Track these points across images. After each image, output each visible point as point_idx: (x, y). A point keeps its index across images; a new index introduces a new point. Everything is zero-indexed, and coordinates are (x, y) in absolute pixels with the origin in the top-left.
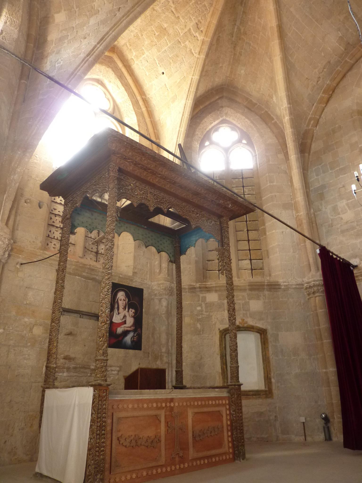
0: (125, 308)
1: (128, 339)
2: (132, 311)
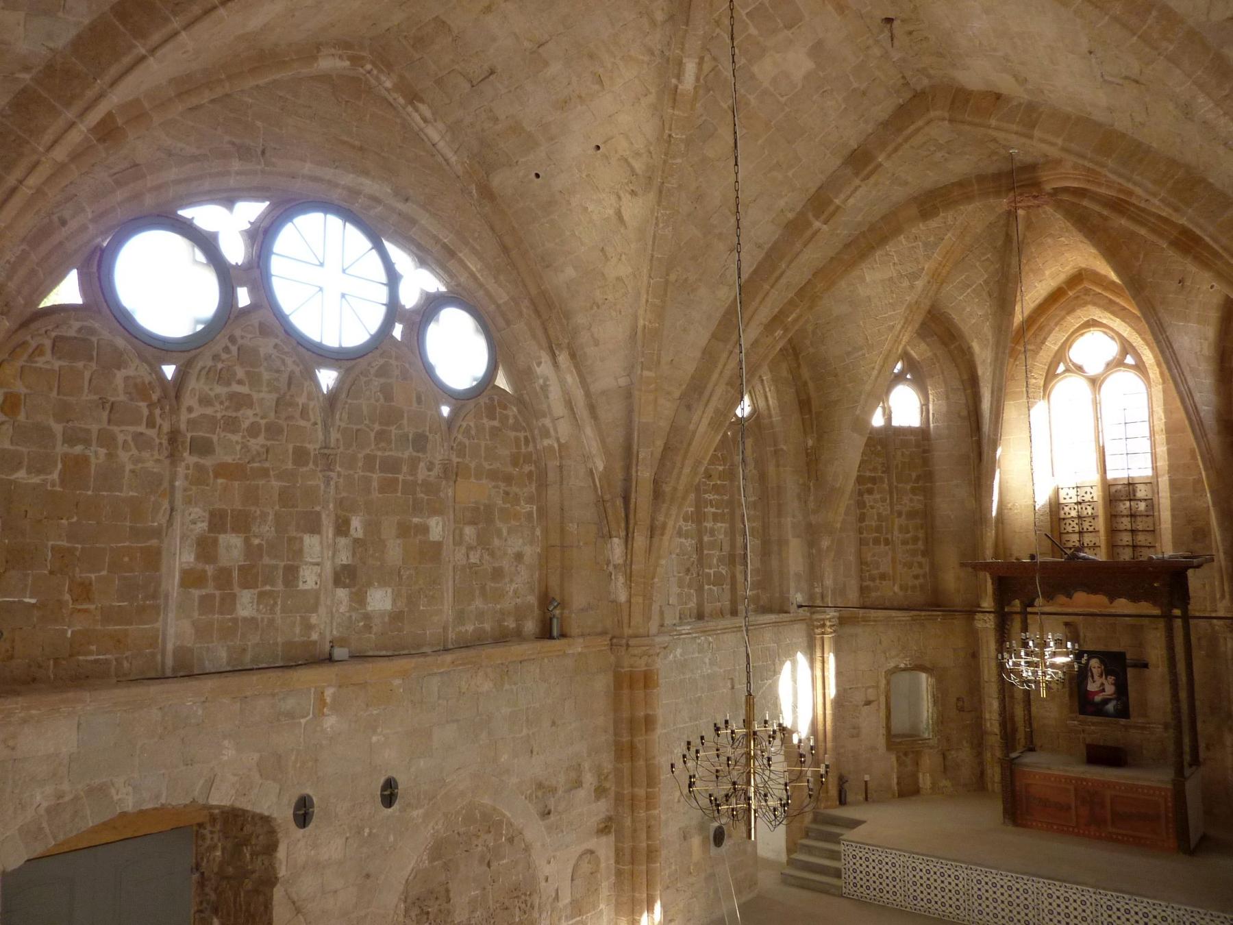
0: (1101, 676)
1: (1110, 707)
2: (1111, 679)
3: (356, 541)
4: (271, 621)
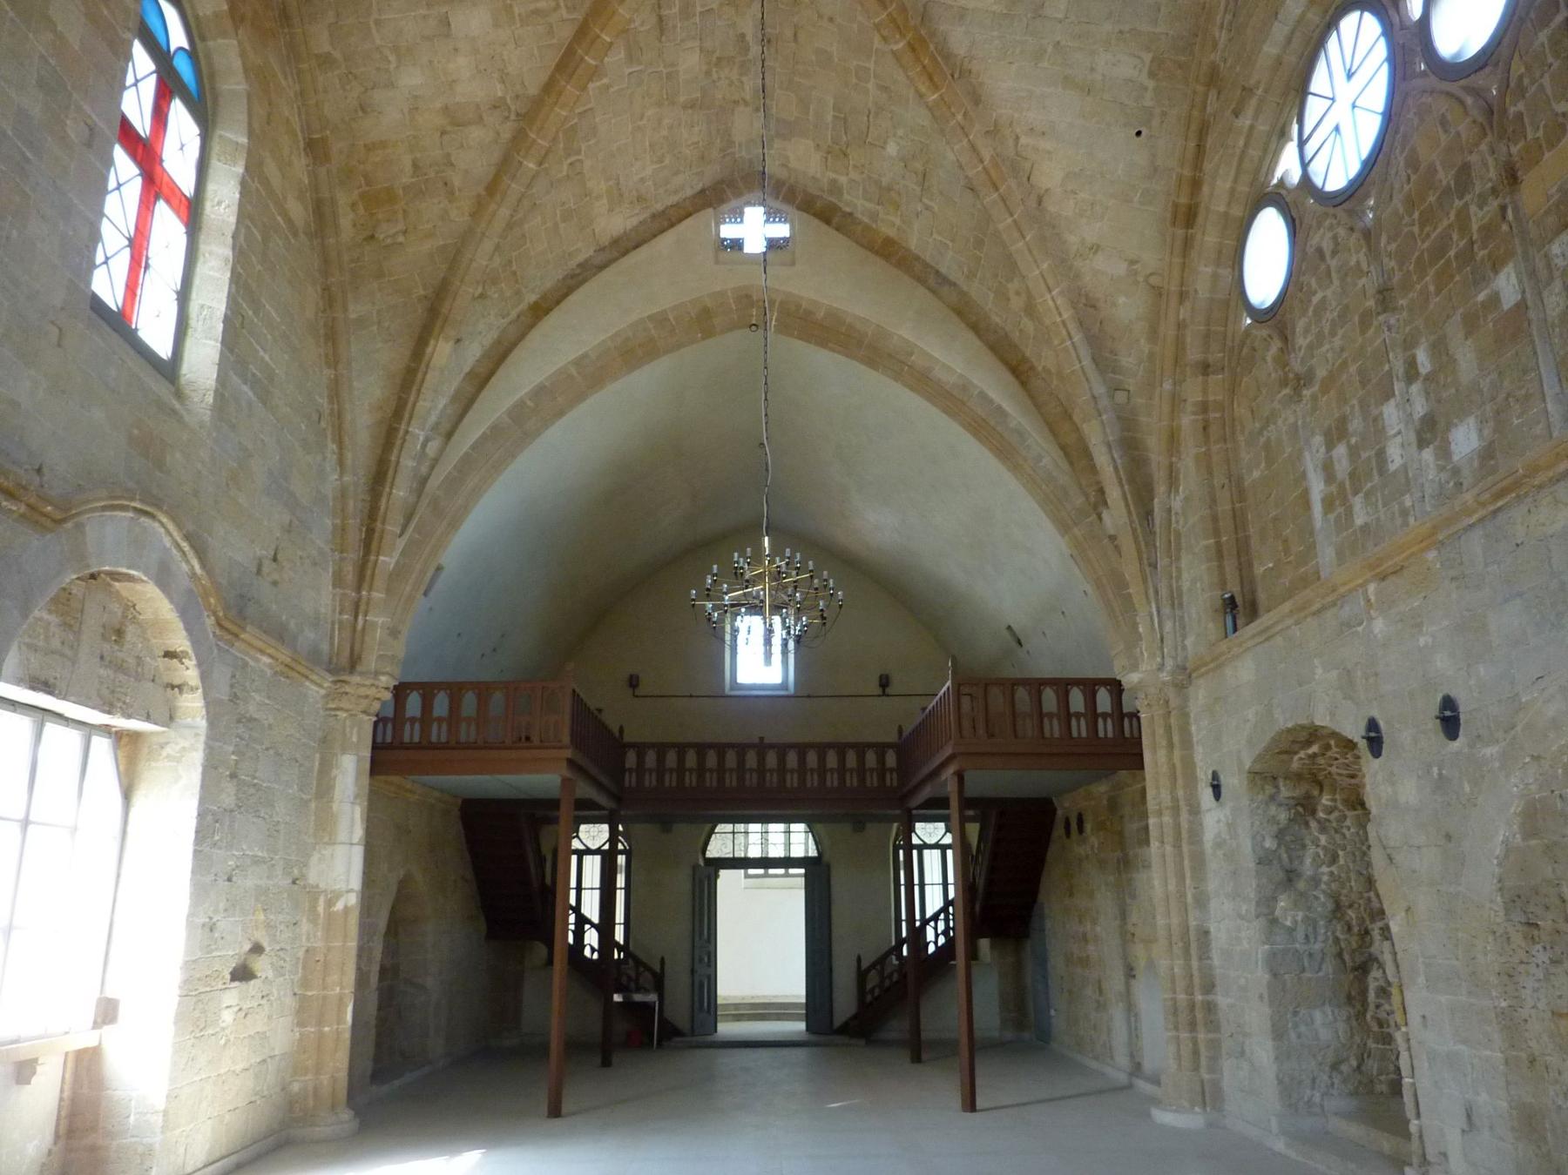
3: (1427, 378)
4: (1378, 519)
